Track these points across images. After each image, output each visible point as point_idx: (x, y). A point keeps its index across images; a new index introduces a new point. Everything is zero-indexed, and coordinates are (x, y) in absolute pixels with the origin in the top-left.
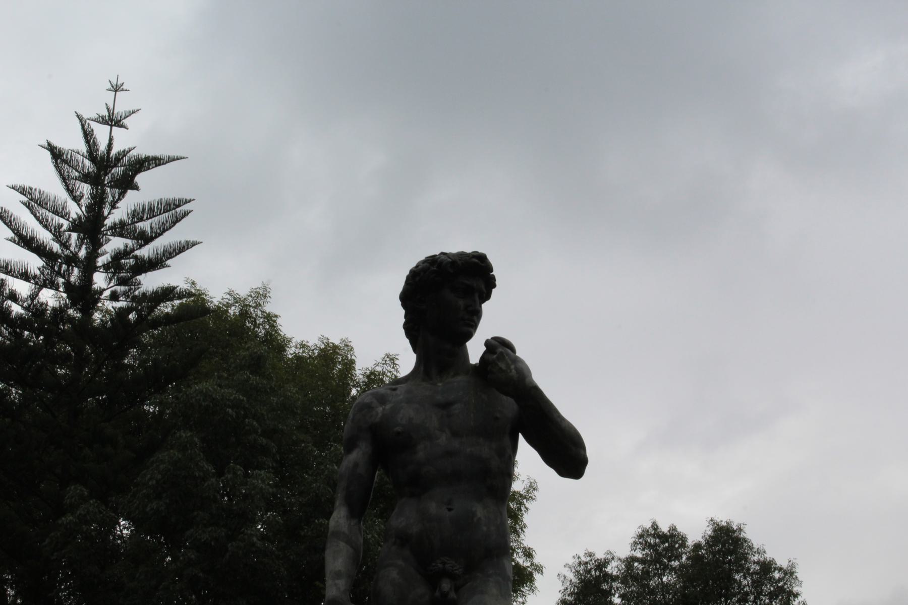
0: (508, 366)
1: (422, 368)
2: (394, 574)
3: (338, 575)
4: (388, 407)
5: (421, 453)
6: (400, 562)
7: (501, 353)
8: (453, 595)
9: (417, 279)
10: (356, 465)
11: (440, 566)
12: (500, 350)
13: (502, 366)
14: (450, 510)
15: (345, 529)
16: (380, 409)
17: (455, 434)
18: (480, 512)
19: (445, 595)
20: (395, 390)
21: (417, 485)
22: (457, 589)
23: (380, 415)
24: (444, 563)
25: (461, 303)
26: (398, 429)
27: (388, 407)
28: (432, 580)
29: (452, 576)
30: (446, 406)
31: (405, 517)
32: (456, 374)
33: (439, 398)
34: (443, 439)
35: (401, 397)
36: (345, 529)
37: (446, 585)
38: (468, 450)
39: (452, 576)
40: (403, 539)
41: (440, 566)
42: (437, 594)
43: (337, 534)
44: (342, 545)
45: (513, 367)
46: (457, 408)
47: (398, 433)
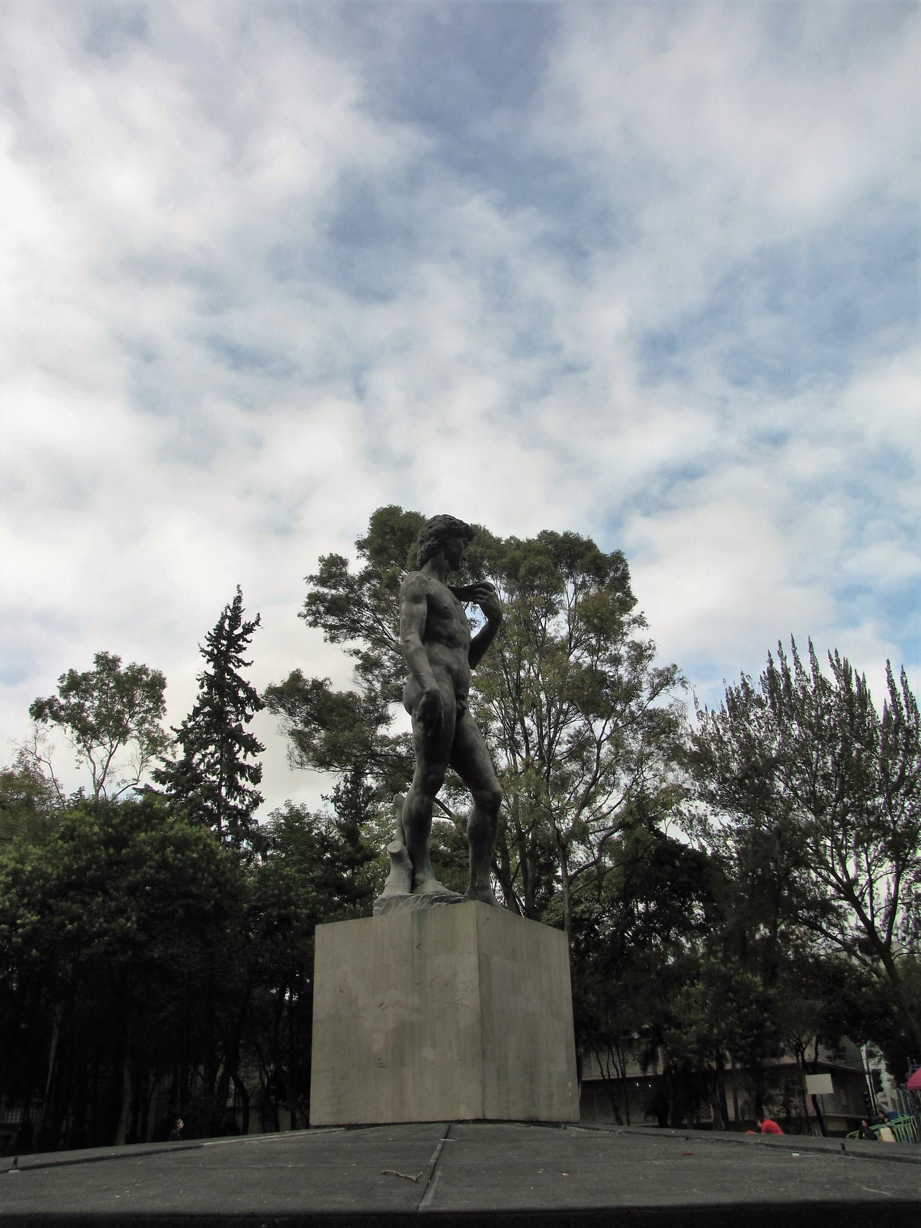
40: (449, 670)
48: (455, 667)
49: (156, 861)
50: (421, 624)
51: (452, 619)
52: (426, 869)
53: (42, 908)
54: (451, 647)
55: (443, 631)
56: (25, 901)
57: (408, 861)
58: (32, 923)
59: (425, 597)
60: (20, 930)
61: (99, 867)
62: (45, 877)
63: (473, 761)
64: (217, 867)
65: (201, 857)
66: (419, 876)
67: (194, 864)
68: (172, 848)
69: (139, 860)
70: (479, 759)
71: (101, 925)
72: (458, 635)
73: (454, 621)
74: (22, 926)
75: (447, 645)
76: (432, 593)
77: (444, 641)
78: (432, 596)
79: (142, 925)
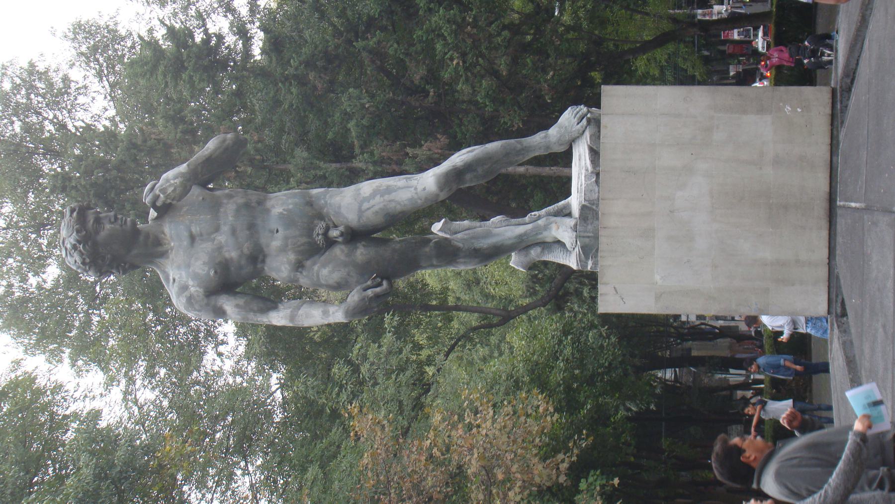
0: (171, 185)
1: (158, 260)
2: (325, 272)
3: (326, 313)
4: (191, 283)
6: (316, 268)
7: (160, 191)
8: (342, 228)
9: (88, 260)
10: (237, 306)
11: (320, 237)
12: (157, 192)
13: (170, 190)
14: (277, 231)
15: (289, 311)
16: (192, 289)
17: (217, 229)
18: (277, 210)
19: (342, 234)
20: (174, 280)
21: (257, 257)
22: (336, 226)
23: (198, 289)
24: (318, 235)
25: (108, 226)
26: (212, 273)
27: (191, 283)
28: (330, 243)
29: (327, 229)
30: (192, 238)
31: (279, 268)
32: (163, 233)
34: (222, 238)
35: (184, 274)
36: (289, 311)
37: (334, 233)
38: (231, 219)
39: (327, 229)
40: (299, 266)
41: (320, 237)
42: (340, 239)
43: (292, 318)
44: (300, 312)
45: (172, 182)
46: (195, 229)
47: (216, 272)
48: (292, 257)
50: (254, 312)
51: (226, 260)
52: (540, 236)
54: (265, 256)
55: (247, 270)
57: (535, 254)
59: (213, 298)
66: (549, 240)
70: (399, 208)
72: (246, 251)
73: (227, 255)
75: (263, 261)
76: (201, 290)
77: (259, 266)
78: (205, 292)
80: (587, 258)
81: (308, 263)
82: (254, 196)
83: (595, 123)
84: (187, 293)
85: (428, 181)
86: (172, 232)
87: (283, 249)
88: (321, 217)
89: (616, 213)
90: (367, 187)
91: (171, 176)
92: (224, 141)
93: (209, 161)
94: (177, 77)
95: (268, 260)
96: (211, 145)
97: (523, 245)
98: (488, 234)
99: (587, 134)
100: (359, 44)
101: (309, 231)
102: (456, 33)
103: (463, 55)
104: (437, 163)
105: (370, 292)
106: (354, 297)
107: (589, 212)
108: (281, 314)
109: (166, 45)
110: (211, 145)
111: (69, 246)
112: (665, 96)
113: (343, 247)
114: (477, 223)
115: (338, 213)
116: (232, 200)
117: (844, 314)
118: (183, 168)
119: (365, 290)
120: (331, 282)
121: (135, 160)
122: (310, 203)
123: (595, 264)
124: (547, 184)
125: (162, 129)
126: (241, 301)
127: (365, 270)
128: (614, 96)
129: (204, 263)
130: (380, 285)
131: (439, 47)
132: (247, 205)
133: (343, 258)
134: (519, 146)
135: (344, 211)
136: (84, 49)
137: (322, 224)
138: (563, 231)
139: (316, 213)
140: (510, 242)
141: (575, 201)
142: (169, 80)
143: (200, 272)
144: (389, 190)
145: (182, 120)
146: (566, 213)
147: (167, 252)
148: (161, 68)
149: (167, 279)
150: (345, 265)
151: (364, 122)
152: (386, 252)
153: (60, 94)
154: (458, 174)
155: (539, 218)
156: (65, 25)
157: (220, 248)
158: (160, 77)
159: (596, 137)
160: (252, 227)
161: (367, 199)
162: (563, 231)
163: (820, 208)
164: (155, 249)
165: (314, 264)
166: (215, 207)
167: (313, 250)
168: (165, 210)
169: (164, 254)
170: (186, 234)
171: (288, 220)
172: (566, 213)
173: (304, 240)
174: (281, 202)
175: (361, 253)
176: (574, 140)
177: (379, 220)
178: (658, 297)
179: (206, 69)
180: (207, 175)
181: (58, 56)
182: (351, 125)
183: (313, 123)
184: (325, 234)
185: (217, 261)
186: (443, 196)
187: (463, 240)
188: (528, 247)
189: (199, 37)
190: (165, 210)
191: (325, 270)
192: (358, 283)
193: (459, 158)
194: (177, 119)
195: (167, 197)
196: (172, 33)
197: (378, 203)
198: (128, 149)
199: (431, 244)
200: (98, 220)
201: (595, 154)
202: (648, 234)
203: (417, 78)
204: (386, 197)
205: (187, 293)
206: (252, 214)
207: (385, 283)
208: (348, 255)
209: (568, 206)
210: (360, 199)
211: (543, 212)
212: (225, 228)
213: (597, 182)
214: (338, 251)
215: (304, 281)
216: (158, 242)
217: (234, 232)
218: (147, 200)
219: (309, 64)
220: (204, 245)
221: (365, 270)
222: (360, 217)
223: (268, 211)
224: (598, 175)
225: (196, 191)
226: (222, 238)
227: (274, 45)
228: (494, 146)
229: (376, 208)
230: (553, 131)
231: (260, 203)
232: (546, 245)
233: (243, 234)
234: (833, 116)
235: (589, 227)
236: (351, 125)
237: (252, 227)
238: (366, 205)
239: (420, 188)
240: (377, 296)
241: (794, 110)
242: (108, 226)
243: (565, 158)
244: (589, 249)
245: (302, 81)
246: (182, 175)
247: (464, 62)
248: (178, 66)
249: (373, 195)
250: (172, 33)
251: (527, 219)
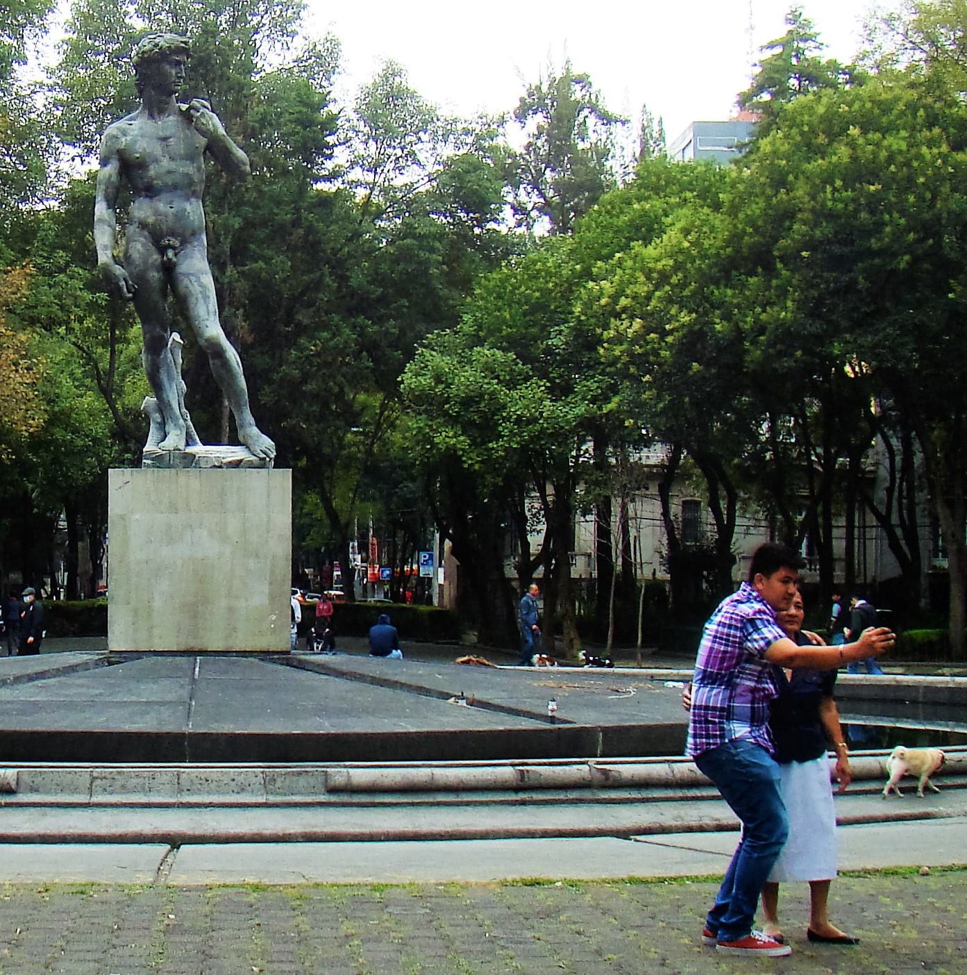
2: (139, 246)
4: (129, 138)
5: (152, 173)
6: (142, 239)
8: (174, 259)
10: (110, 176)
13: (203, 120)
15: (106, 217)
16: (123, 139)
17: (172, 159)
18: (188, 208)
21: (151, 191)
22: (176, 255)
27: (129, 138)
28: (162, 250)
29: (174, 248)
30: (165, 139)
31: (141, 209)
33: (161, 134)
34: (166, 163)
35: (136, 132)
36: (106, 217)
37: (170, 253)
39: (174, 248)
40: (143, 225)
43: (100, 220)
44: (106, 228)
48: (151, 220)
49: (813, 210)
53: (702, 303)
54: (151, 198)
55: (140, 184)
56: (686, 292)
57: (156, 417)
58: (683, 325)
59: (116, 156)
60: (670, 339)
61: (756, 229)
62: (703, 256)
63: (187, 309)
64: (920, 198)
65: (886, 187)
67: (873, 204)
68: (838, 183)
69: (789, 214)
71: (757, 320)
73: (151, 167)
74: (671, 332)
75: (147, 196)
76: (122, 147)
79: (813, 309)
80: (152, 459)
81: (146, 233)
82: (200, 188)
83: (262, 464)
84: (120, 135)
85: (213, 329)
86: (170, 123)
87: (156, 213)
88: (184, 242)
89: (188, 481)
90: (208, 280)
91: (214, 123)
92: (244, 164)
93: (227, 152)
94: (297, 121)
95: (147, 200)
96: (241, 154)
97: (163, 407)
98: (170, 378)
99: (253, 458)
100: (326, 269)
101: (173, 234)
102: (336, 347)
103: (318, 354)
104: (228, 336)
105: (124, 283)
106: (118, 270)
107: (189, 461)
108: (104, 211)
109: (324, 112)
110: (241, 154)
111: (157, 41)
112: (283, 519)
113: (159, 260)
114: (179, 371)
115: (186, 257)
116: (195, 170)
117: (110, 664)
118: (222, 131)
119: (125, 279)
120: (131, 252)
121: (230, 88)
122: (194, 234)
123: (148, 466)
124: (213, 426)
125: (255, 111)
126: (114, 179)
127: (140, 278)
128: (283, 479)
129: (144, 149)
130: (129, 291)
131: (325, 334)
132: (191, 183)
133: (150, 261)
134: (242, 403)
135: (188, 262)
136: (319, 48)
137: (177, 244)
138: (175, 439)
139: (186, 238)
140: (165, 396)
141: (199, 449)
142: (295, 115)
143: (137, 146)
144: (206, 298)
145: (263, 127)
146: (189, 441)
147: (153, 118)
148: (305, 110)
149: (131, 119)
150: (145, 262)
151: (263, 274)
152: (156, 296)
153: (283, 30)
154: (219, 353)
155: (185, 420)
156: (338, 33)
157: (156, 161)
158: (297, 109)
159: (251, 465)
160: (175, 187)
161: (198, 279)
162: (175, 439)
163: (195, 644)
164: (156, 109)
165: (145, 238)
166: (191, 157)
167: (157, 236)
168: (187, 117)
169: (151, 116)
170: (168, 134)
171: (180, 216)
172: (189, 441)
173: (164, 227)
174: (195, 211)
175: (154, 276)
176: (247, 447)
177: (182, 289)
178: (122, 517)
179: (305, 144)
180: (215, 149)
181: (313, 27)
182: (261, 264)
183: (261, 233)
184: (170, 247)
185: (148, 160)
186: (202, 342)
187: (166, 357)
188: (161, 411)
189: (331, 140)
190: (187, 117)
191: (140, 247)
192: (130, 274)
193: (232, 354)
194: (264, 121)
195: (197, 118)
196: (333, 118)
197: (195, 289)
198: (239, 84)
199: (162, 333)
200: (178, 63)
201: (237, 464)
202: (173, 508)
203: (299, 317)
204: (200, 296)
205: (120, 135)
206: (184, 188)
207: (131, 295)
208: (152, 264)
209: (195, 444)
210: (197, 271)
211: (190, 423)
212: (173, 165)
213: (215, 466)
214: (156, 257)
215: (131, 229)
216: (162, 111)
217: (169, 172)
218: (195, 102)
219: (310, 230)
220: (159, 148)
221: (140, 278)
222: (184, 274)
223: (188, 200)
224: (220, 467)
225: (203, 141)
226: (166, 163)
227: (325, 201)
228: (242, 382)
229: (191, 288)
230: (255, 430)
231: (194, 194)
232: (162, 425)
233: (169, 180)
234: (268, 653)
235: (177, 461)
236: (261, 264)
237: (175, 187)
238: (193, 279)
239: (208, 323)
240: (120, 289)
241: (273, 622)
242: (174, 72)
243: (234, 441)
244: (160, 461)
245: (296, 223)
246: (216, 130)
247: (313, 355)
248: (307, 123)
249: (201, 285)
250: (333, 118)
251: (184, 410)
